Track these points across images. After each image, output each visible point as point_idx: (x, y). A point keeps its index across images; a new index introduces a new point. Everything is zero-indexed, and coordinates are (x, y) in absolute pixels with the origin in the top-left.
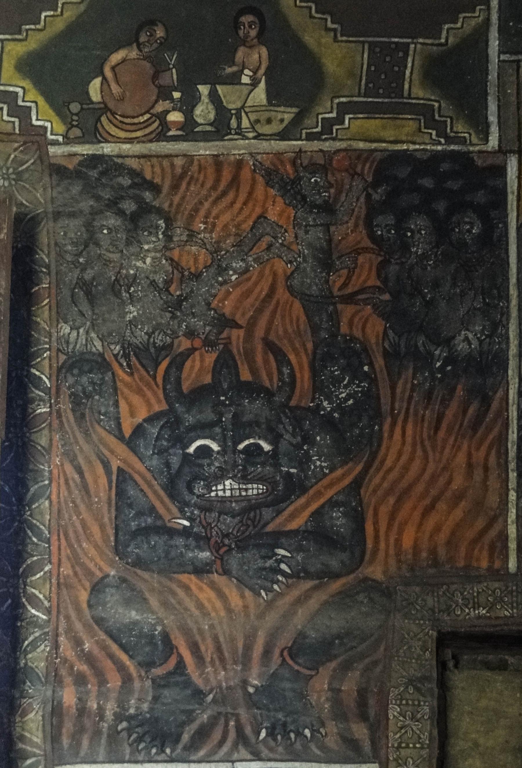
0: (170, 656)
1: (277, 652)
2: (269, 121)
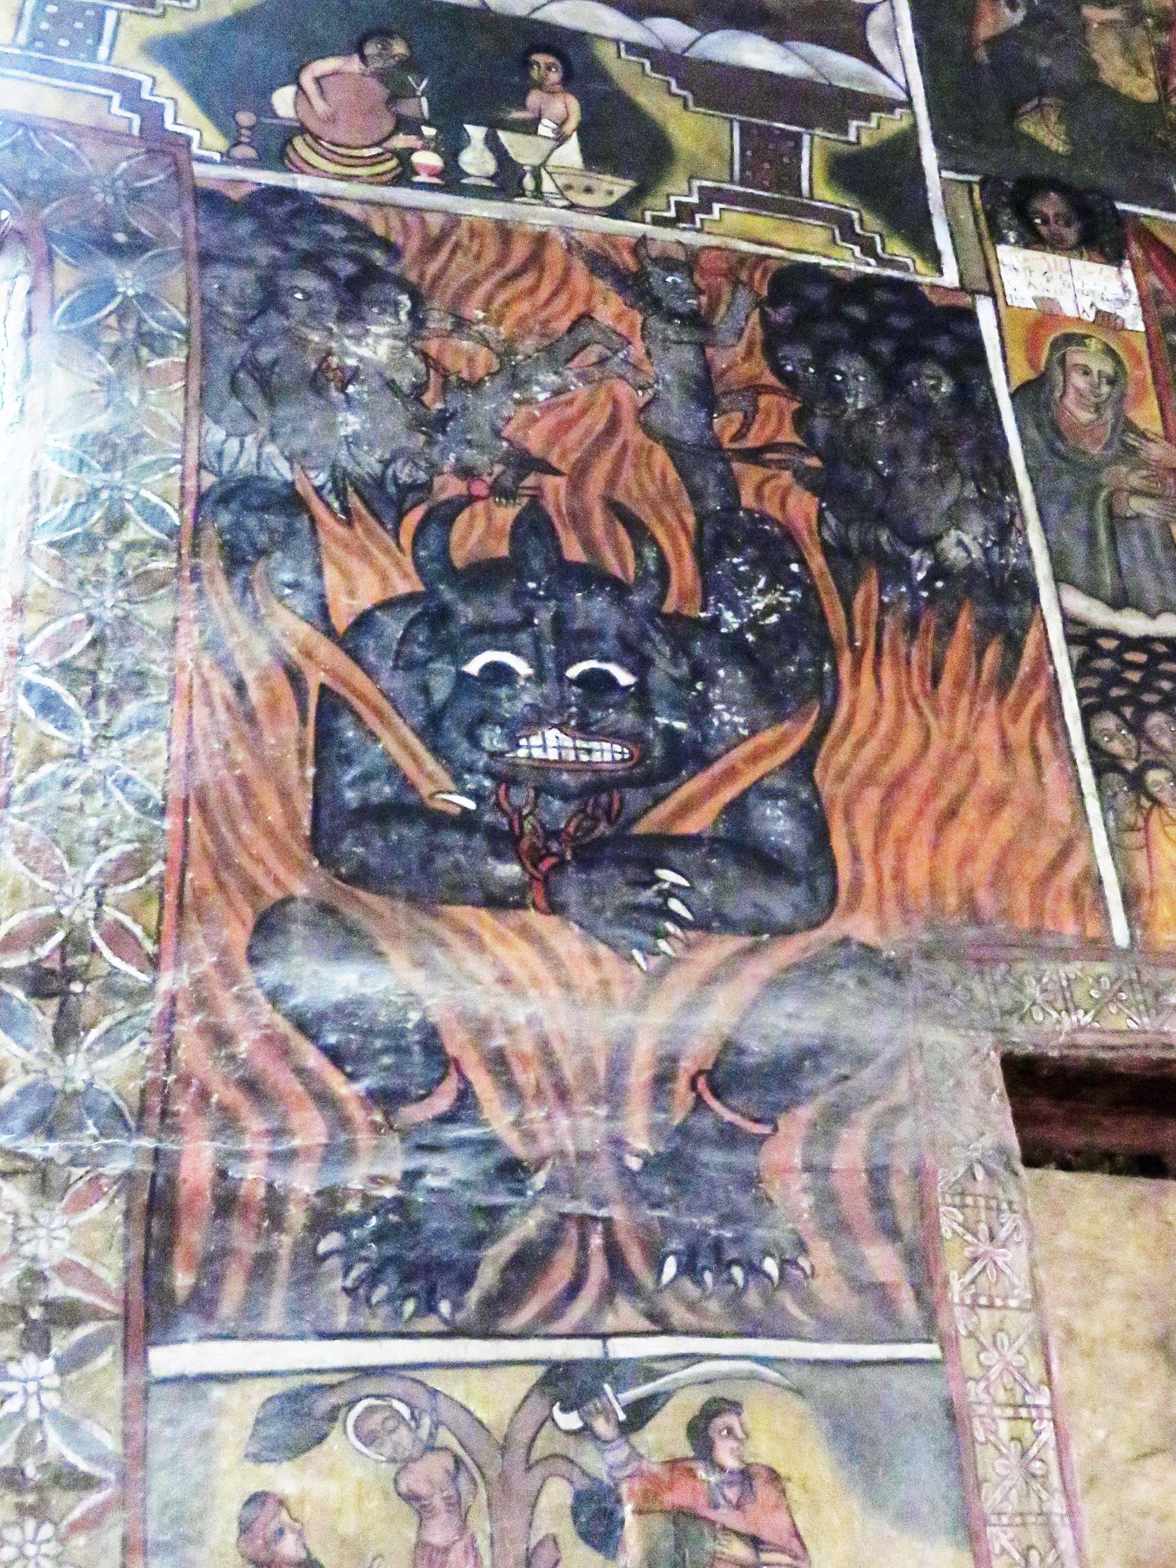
0: (440, 1081)
1: (682, 1084)
2: (588, 190)
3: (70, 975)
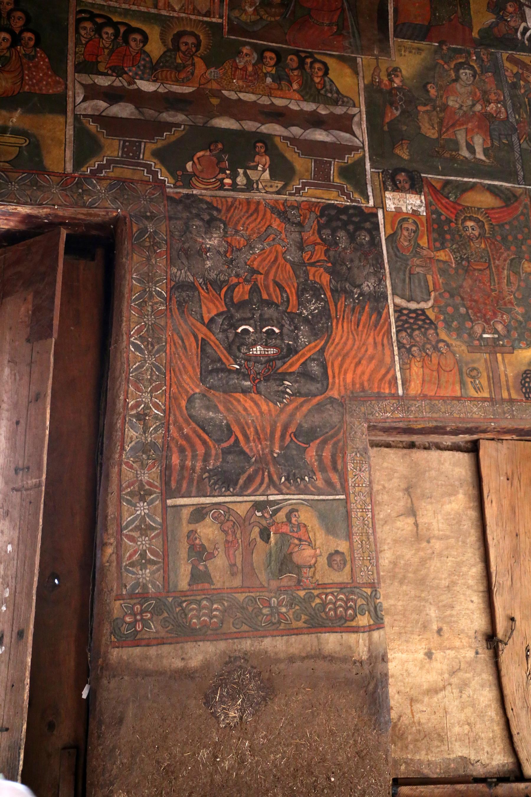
2: (271, 186)
3: (146, 415)
